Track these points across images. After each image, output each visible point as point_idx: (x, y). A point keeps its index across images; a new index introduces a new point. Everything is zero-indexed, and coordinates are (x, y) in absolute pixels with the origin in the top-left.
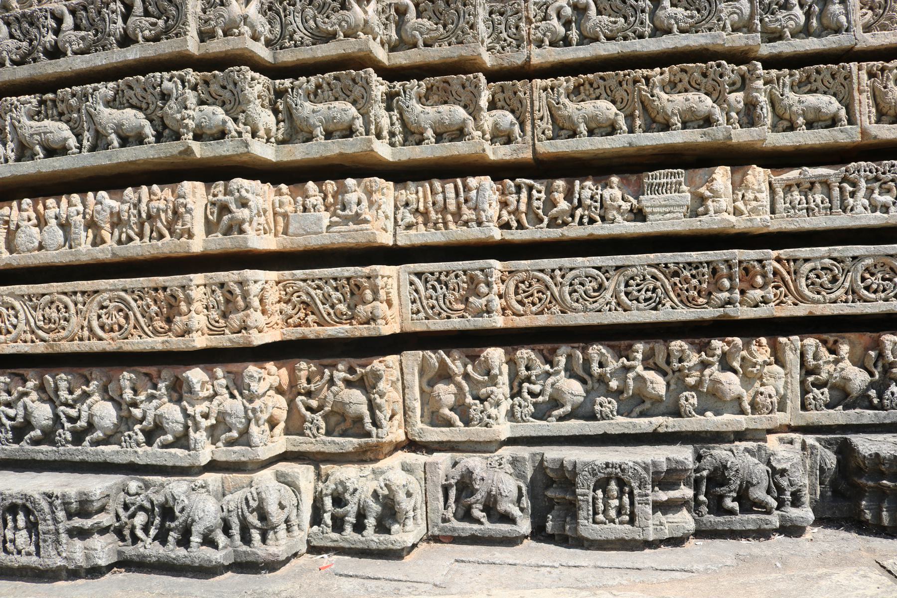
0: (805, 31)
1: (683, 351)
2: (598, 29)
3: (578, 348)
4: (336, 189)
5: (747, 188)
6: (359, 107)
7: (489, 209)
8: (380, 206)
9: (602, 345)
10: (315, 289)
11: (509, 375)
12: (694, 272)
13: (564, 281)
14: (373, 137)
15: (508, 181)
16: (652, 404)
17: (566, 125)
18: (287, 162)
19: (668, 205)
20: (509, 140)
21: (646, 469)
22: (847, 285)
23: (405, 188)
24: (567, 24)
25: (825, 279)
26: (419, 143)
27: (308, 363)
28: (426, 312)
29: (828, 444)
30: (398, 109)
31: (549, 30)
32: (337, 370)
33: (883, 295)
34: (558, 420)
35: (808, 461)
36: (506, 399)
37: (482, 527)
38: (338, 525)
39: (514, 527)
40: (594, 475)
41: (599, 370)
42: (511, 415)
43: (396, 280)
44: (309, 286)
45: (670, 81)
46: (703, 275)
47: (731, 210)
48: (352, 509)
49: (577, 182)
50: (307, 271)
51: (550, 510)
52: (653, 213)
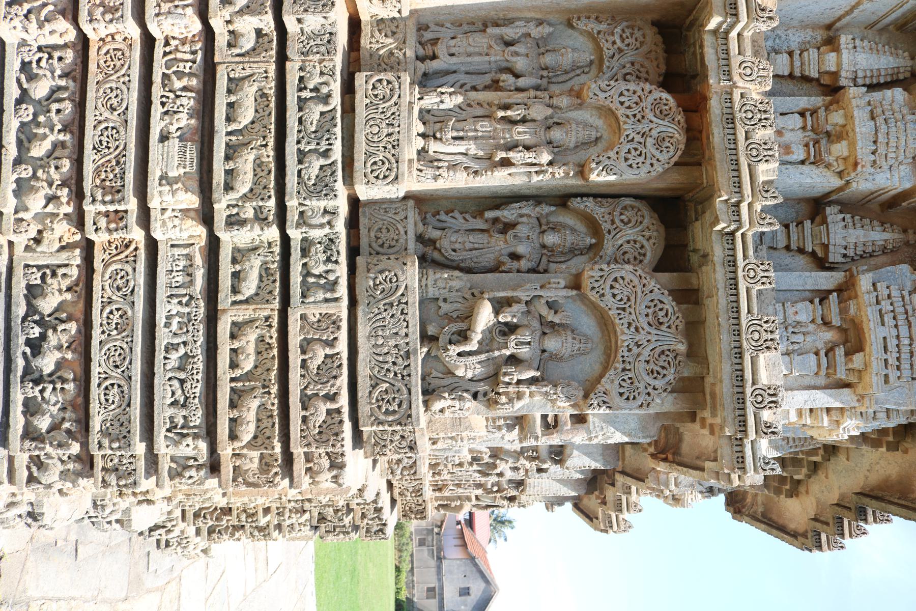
0: (307, 274)
5: (182, 220)
15: (199, 46)
22: (114, 297)
24: (316, 89)
25: (119, 282)
31: (311, 75)
33: (105, 322)
49: (193, 95)
52: (163, 147)
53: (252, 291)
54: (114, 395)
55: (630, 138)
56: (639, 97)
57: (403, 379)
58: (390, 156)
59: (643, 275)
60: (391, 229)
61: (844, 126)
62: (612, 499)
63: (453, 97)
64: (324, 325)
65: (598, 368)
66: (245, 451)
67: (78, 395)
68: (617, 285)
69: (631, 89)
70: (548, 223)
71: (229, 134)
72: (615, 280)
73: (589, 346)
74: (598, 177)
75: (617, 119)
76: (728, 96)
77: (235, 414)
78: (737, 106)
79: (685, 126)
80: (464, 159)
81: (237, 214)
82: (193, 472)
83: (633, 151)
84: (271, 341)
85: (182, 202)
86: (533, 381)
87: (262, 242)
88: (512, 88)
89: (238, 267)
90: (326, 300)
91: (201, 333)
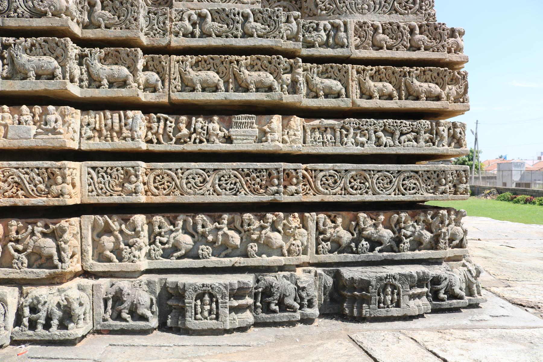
0: (326, 45)
1: (250, 220)
2: (212, 30)
3: (190, 216)
4: (41, 111)
5: (290, 128)
6: (60, 61)
7: (140, 130)
8: (70, 125)
9: (204, 214)
10: (24, 174)
11: (149, 231)
12: (258, 174)
13: (183, 176)
14: (68, 81)
16: (232, 250)
17: (189, 84)
18: (9, 91)
19: (245, 135)
20: (155, 90)
21: (226, 287)
22: (342, 185)
23: (88, 114)
24: (194, 25)
25: (331, 181)
26: (98, 87)
27: (17, 221)
28: (97, 192)
29: (329, 273)
30: (86, 65)
31: (183, 27)
32: (37, 226)
33: (360, 192)
34: (176, 259)
35: (318, 283)
36: (146, 246)
37: (127, 324)
38: (33, 325)
39: (147, 323)
40: (196, 291)
41: (202, 230)
42: (149, 256)
43: (79, 171)
44: (20, 172)
45: (250, 64)
46: (263, 176)
47: (281, 140)
48: (42, 315)
49: (194, 118)
50: (19, 162)
51: (170, 312)
52: (236, 139)
54: (410, 183)
64: (363, 33)
90: (346, 31)
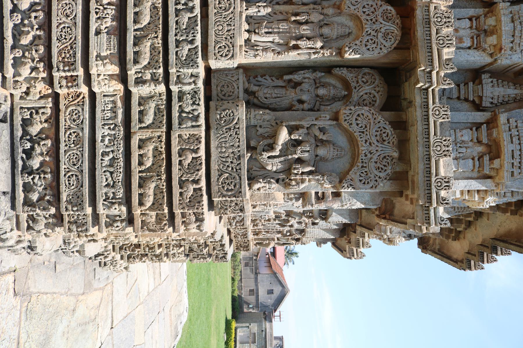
0: (181, 111)
5: (109, 80)
22: (72, 126)
25: (75, 117)
33: (67, 140)
45: (155, 47)
47: (99, 72)
49: (114, 7)
52: (97, 38)
53: (150, 121)
54: (73, 181)
55: (369, 33)
56: (374, 8)
57: (236, 171)
58: (229, 43)
59: (374, 113)
60: (229, 85)
61: (495, 26)
62: (354, 240)
63: (266, 9)
64: (191, 141)
65: (347, 166)
66: (148, 212)
67: (53, 181)
68: (359, 119)
69: (370, 4)
70: (320, 83)
71: (135, 30)
72: (358, 115)
73: (343, 153)
74: (350, 56)
75: (361, 22)
76: (427, 8)
77: (142, 191)
78: (432, 14)
79: (401, 26)
80: (272, 45)
81: (141, 77)
82: (119, 224)
83: (370, 41)
84: (161, 150)
85: (109, 70)
86: (310, 173)
87: (155, 93)
88: (300, 3)
89: (142, 108)
90: (193, 127)
91: (122, 145)
